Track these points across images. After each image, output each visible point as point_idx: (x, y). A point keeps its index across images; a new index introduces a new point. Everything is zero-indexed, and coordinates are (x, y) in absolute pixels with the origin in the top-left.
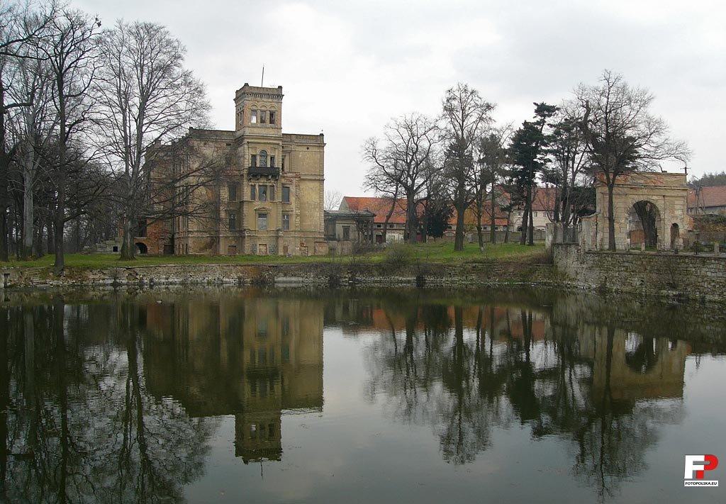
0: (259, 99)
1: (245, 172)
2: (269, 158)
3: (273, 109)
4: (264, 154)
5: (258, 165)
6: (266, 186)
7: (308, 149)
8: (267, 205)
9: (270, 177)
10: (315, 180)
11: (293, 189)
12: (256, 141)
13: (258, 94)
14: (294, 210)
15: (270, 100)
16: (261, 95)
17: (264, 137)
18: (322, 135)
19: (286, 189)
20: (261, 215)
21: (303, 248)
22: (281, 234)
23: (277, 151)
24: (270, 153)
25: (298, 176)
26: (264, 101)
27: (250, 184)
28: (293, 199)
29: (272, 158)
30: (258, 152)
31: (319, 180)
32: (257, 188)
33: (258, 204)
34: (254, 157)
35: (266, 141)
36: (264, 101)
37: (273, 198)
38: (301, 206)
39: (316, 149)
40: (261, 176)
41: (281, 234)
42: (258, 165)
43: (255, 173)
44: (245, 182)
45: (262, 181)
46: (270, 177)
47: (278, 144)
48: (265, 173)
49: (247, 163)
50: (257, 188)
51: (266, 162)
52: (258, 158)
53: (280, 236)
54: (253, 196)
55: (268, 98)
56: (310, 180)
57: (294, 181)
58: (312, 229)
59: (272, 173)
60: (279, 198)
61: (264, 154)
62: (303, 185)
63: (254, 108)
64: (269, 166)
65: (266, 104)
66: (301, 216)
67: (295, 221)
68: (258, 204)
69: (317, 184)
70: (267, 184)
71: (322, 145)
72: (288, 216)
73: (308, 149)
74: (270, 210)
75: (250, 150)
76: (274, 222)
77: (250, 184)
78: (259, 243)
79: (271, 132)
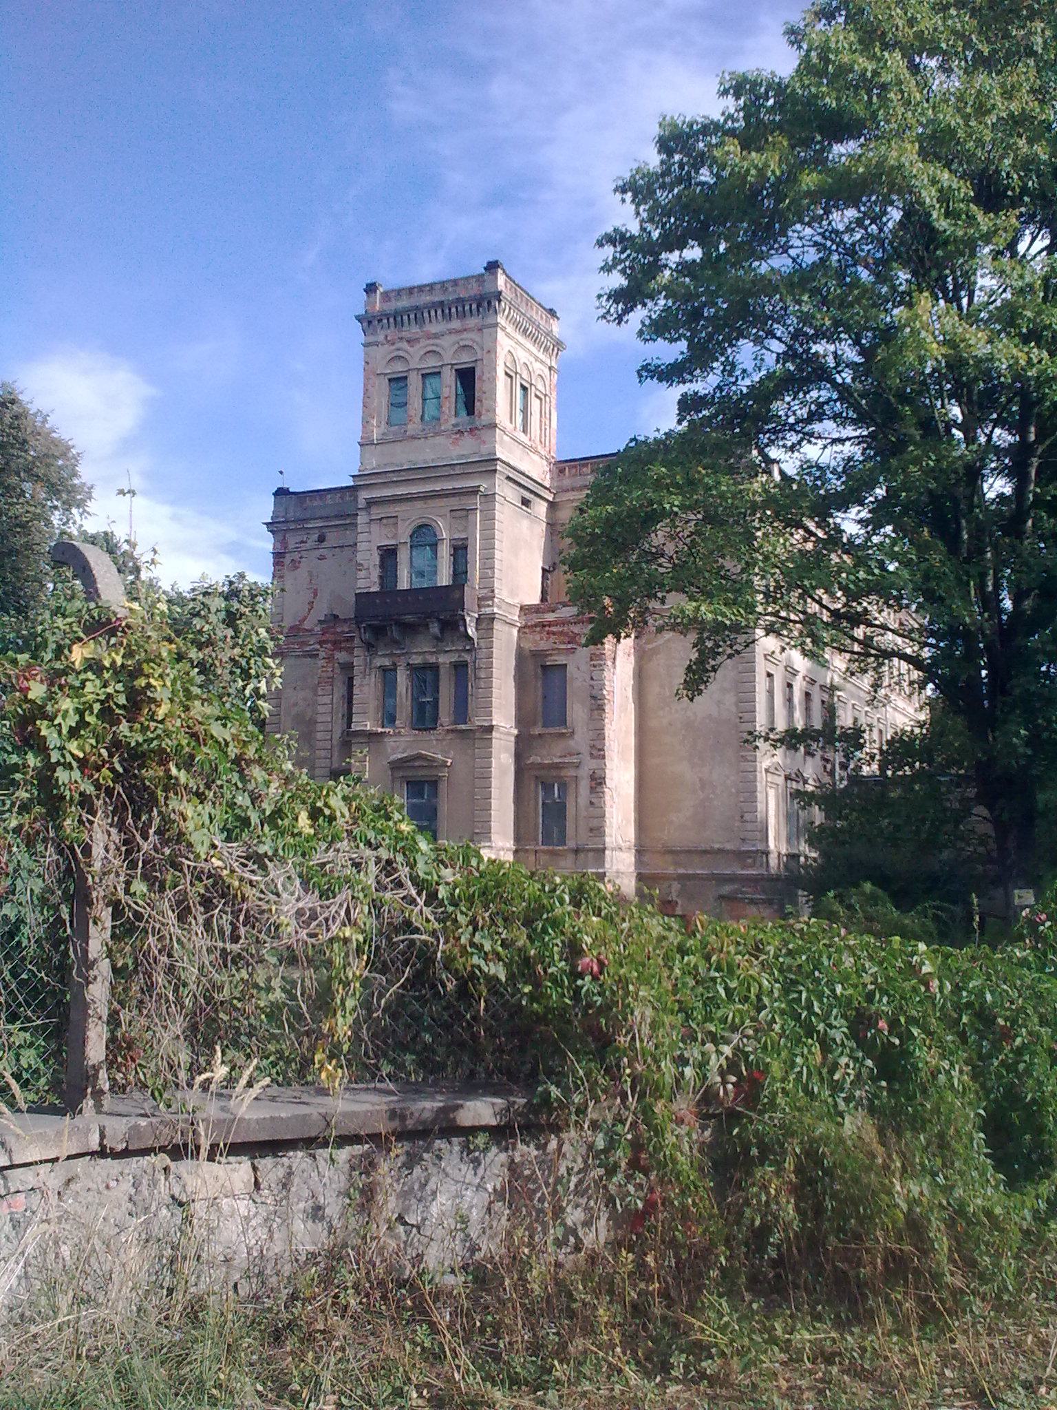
2: (445, 551)
3: (465, 359)
5: (404, 584)
6: (435, 668)
13: (407, 311)
15: (456, 324)
16: (418, 314)
24: (445, 533)
29: (460, 551)
32: (402, 680)
33: (403, 743)
34: (388, 555)
36: (429, 336)
40: (410, 629)
42: (404, 584)
45: (421, 651)
47: (474, 491)
50: (402, 680)
52: (403, 556)
61: (424, 536)
63: (399, 367)
64: (444, 578)
65: (445, 343)
70: (442, 659)
72: (564, 787)
75: (375, 527)
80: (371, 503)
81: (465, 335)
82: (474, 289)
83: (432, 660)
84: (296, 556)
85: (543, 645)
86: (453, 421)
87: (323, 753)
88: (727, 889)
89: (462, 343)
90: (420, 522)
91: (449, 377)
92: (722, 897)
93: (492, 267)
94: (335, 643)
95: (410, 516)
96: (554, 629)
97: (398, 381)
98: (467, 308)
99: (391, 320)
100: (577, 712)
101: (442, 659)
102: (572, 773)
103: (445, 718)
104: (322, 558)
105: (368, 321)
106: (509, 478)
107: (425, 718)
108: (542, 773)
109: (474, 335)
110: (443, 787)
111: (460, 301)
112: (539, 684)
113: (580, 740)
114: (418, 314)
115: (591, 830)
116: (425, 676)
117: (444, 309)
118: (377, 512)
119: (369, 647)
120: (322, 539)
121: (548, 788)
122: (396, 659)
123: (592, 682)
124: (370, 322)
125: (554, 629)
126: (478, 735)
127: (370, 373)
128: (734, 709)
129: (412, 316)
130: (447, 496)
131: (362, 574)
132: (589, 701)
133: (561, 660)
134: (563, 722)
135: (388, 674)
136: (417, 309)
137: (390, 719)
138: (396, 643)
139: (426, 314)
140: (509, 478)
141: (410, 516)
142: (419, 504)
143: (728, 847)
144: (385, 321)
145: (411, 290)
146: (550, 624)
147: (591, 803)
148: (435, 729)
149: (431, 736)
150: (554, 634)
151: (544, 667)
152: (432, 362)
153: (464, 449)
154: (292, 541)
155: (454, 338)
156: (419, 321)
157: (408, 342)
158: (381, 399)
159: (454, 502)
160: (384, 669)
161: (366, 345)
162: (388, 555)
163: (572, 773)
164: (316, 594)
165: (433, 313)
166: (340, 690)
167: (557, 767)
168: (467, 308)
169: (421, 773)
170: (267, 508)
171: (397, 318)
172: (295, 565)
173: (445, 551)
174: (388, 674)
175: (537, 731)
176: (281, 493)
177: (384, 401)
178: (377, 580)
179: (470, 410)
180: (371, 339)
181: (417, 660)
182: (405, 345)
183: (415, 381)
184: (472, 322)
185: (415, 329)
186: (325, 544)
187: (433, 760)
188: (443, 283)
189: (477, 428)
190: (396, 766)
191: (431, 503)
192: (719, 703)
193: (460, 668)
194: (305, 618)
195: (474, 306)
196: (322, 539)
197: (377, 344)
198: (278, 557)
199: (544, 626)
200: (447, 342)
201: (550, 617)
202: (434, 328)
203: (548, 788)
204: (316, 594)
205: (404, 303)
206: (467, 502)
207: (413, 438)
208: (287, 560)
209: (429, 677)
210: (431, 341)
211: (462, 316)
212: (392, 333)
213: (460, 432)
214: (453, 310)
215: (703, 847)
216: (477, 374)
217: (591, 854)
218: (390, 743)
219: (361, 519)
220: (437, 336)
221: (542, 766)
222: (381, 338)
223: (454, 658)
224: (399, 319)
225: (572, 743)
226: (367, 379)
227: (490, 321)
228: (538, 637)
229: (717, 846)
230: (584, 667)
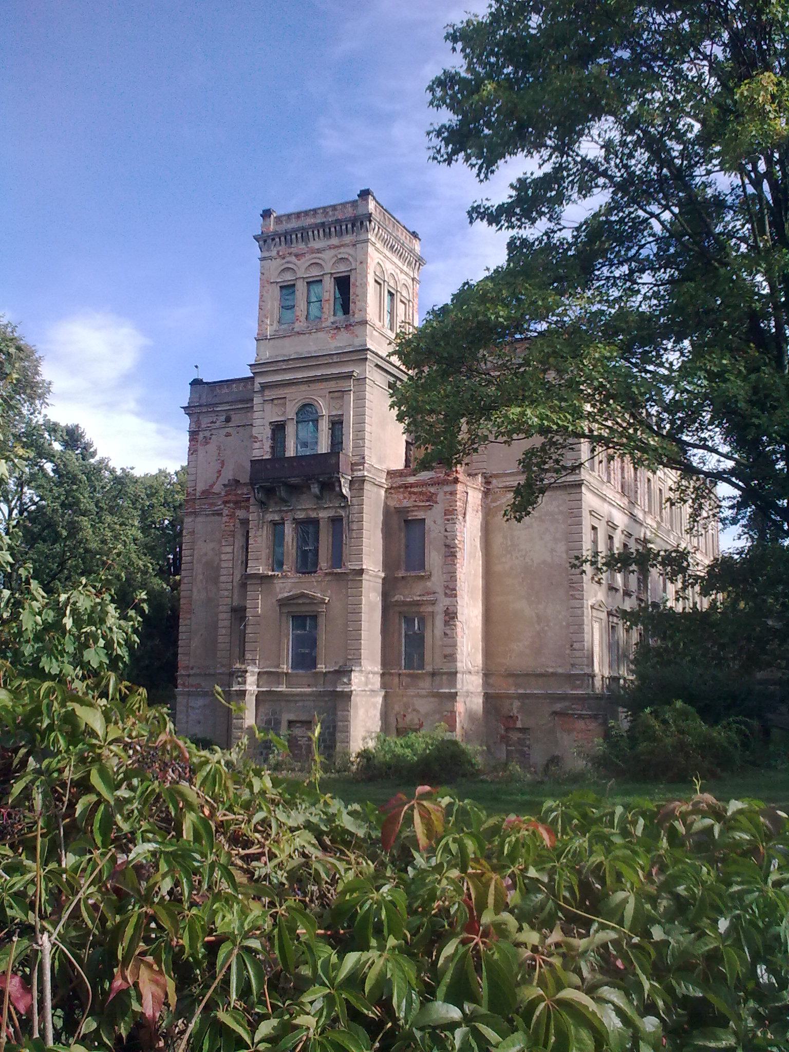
2: (324, 425)
3: (342, 268)
6: (316, 522)
12: (299, 375)
13: (295, 231)
15: (335, 241)
16: (303, 234)
21: (515, 736)
24: (324, 409)
27: (270, 517)
29: (337, 424)
30: (291, 411)
33: (288, 584)
34: (278, 429)
40: (295, 490)
45: (304, 508)
47: (349, 376)
52: (290, 430)
55: (328, 235)
63: (288, 277)
64: (324, 447)
65: (327, 257)
70: (323, 514)
72: (422, 621)
75: (268, 407)
77: (270, 517)
78: (286, 717)
80: (264, 387)
81: (342, 250)
82: (349, 212)
83: (313, 515)
84: (207, 434)
85: (406, 503)
86: (332, 319)
87: (226, 593)
88: (558, 707)
89: (339, 256)
90: (307, 401)
91: (329, 284)
92: (555, 713)
93: (365, 194)
94: (236, 503)
95: (296, 397)
96: (415, 490)
97: (288, 288)
98: (344, 227)
99: (283, 239)
100: (434, 558)
101: (323, 514)
102: (430, 609)
103: (323, 564)
104: (228, 435)
105: (264, 240)
106: (377, 366)
107: (307, 563)
108: (405, 609)
109: (350, 250)
110: (322, 621)
111: (338, 221)
112: (403, 535)
113: (436, 581)
114: (303, 234)
115: (445, 656)
116: (308, 528)
117: (325, 229)
118: (270, 394)
119: (263, 505)
120: (228, 420)
121: (409, 621)
122: (284, 515)
123: (446, 534)
124: (265, 241)
125: (415, 490)
126: (351, 577)
127: (265, 282)
128: (564, 556)
129: (299, 235)
130: (326, 380)
131: (257, 445)
132: (443, 549)
133: (420, 515)
134: (422, 566)
136: (303, 230)
137: (278, 564)
138: (284, 501)
139: (310, 233)
140: (377, 366)
141: (296, 397)
142: (303, 388)
143: (560, 671)
144: (277, 240)
145: (298, 215)
146: (412, 485)
147: (445, 634)
148: (315, 572)
149: (312, 578)
150: (415, 493)
151: (406, 521)
152: (315, 272)
153: (341, 342)
154: (205, 421)
155: (333, 252)
156: (305, 239)
157: (297, 256)
158: (274, 304)
159: (332, 385)
160: (275, 524)
161: (262, 259)
162: (278, 429)
163: (430, 609)
164: (223, 463)
165: (316, 232)
166: (239, 541)
167: (418, 604)
168: (344, 227)
169: (304, 609)
170: (184, 396)
171: (286, 237)
172: (207, 441)
173: (324, 425)
174: (277, 526)
175: (401, 574)
176: (196, 383)
177: (276, 304)
178: (269, 450)
179: (346, 310)
180: (266, 254)
181: (301, 515)
182: (293, 259)
183: (301, 287)
184: (348, 239)
185: (302, 246)
186: (230, 424)
187: (314, 598)
188: (324, 208)
189: (351, 325)
190: (283, 603)
191: (314, 386)
192: (552, 551)
193: (336, 521)
194: (214, 484)
195: (349, 226)
196: (228, 420)
197: (271, 258)
198: (193, 434)
199: (406, 487)
200: (328, 255)
201: (411, 480)
203: (409, 621)
204: (223, 463)
205: (294, 224)
207: (298, 333)
208: (201, 436)
209: (311, 529)
210: (314, 255)
211: (340, 234)
212: (283, 249)
213: (337, 328)
214: (333, 229)
215: (539, 670)
216: (352, 280)
217: (444, 677)
218: (278, 584)
219: (257, 400)
220: (319, 251)
221: (404, 603)
222: (274, 253)
223: (331, 513)
224: (288, 237)
225: (429, 584)
226: (262, 287)
227: (362, 237)
228: (401, 497)
229: (551, 670)
230: (440, 521)
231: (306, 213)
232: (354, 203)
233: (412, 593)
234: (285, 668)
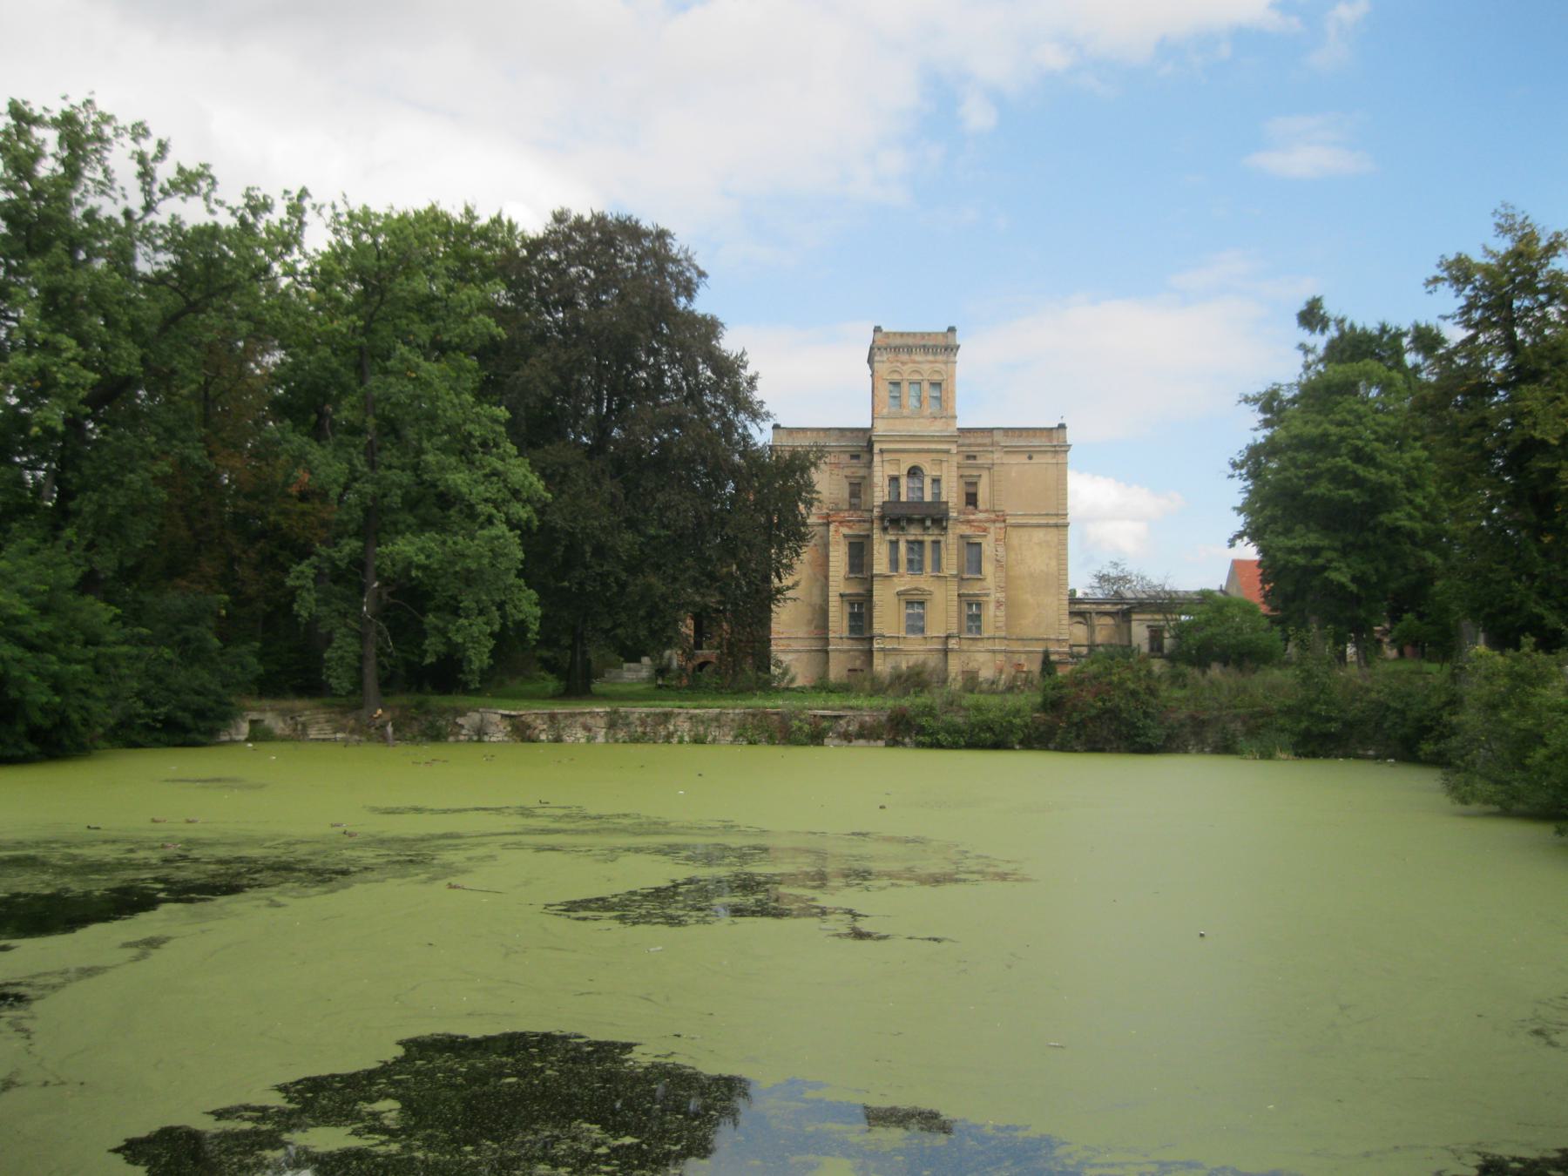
0: (904, 357)
1: (876, 512)
2: (928, 481)
3: (936, 378)
4: (914, 472)
5: (903, 498)
6: (921, 543)
7: (1030, 458)
8: (924, 582)
9: (928, 523)
10: (1047, 526)
11: (988, 548)
14: (992, 592)
15: (930, 358)
16: (909, 349)
17: (914, 438)
18: (1062, 427)
19: (972, 548)
20: (910, 603)
22: (952, 644)
23: (945, 465)
24: (930, 471)
25: (1000, 518)
26: (914, 362)
27: (888, 538)
28: (988, 568)
29: (936, 481)
31: (1056, 526)
32: (903, 547)
33: (904, 581)
34: (894, 480)
35: (925, 446)
36: (914, 362)
37: (937, 564)
38: (1007, 584)
39: (1049, 459)
40: (910, 521)
41: (952, 644)
43: (896, 518)
44: (877, 535)
45: (914, 533)
46: (928, 523)
47: (947, 452)
48: (916, 518)
49: (880, 494)
50: (903, 547)
51: (922, 489)
52: (904, 482)
53: (952, 650)
54: (894, 564)
56: (1039, 526)
57: (992, 530)
58: (1041, 633)
59: (936, 517)
60: (951, 563)
62: (1016, 537)
63: (896, 377)
65: (926, 366)
66: (1010, 605)
67: (991, 614)
68: (904, 581)
69: (1052, 535)
71: (1061, 449)
72: (979, 605)
73: (1030, 458)
74: (931, 593)
76: (942, 615)
77: (888, 538)
79: (936, 428)
80: (882, 451)
82: (941, 341)
95: (907, 463)
101: (928, 539)
107: (915, 565)
110: (928, 605)
117: (925, 349)
118: (887, 457)
119: (885, 529)
135: (894, 545)
138: (903, 529)
145: (902, 334)
152: (917, 377)
159: (934, 456)
160: (891, 542)
171: (897, 349)
173: (928, 481)
174: (894, 545)
181: (911, 538)
183: (905, 385)
184: (940, 358)
190: (899, 594)
193: (936, 543)
202: (918, 358)
203: (970, 605)
205: (898, 341)
206: (941, 456)
209: (916, 547)
211: (935, 354)
219: (877, 459)
231: (909, 334)
232: (944, 334)
233: (974, 589)
234: (903, 634)
